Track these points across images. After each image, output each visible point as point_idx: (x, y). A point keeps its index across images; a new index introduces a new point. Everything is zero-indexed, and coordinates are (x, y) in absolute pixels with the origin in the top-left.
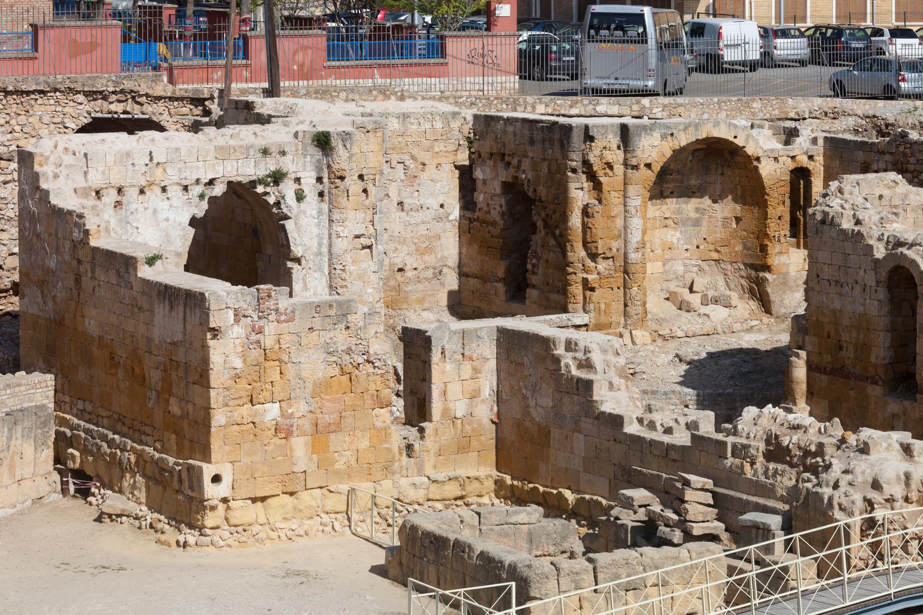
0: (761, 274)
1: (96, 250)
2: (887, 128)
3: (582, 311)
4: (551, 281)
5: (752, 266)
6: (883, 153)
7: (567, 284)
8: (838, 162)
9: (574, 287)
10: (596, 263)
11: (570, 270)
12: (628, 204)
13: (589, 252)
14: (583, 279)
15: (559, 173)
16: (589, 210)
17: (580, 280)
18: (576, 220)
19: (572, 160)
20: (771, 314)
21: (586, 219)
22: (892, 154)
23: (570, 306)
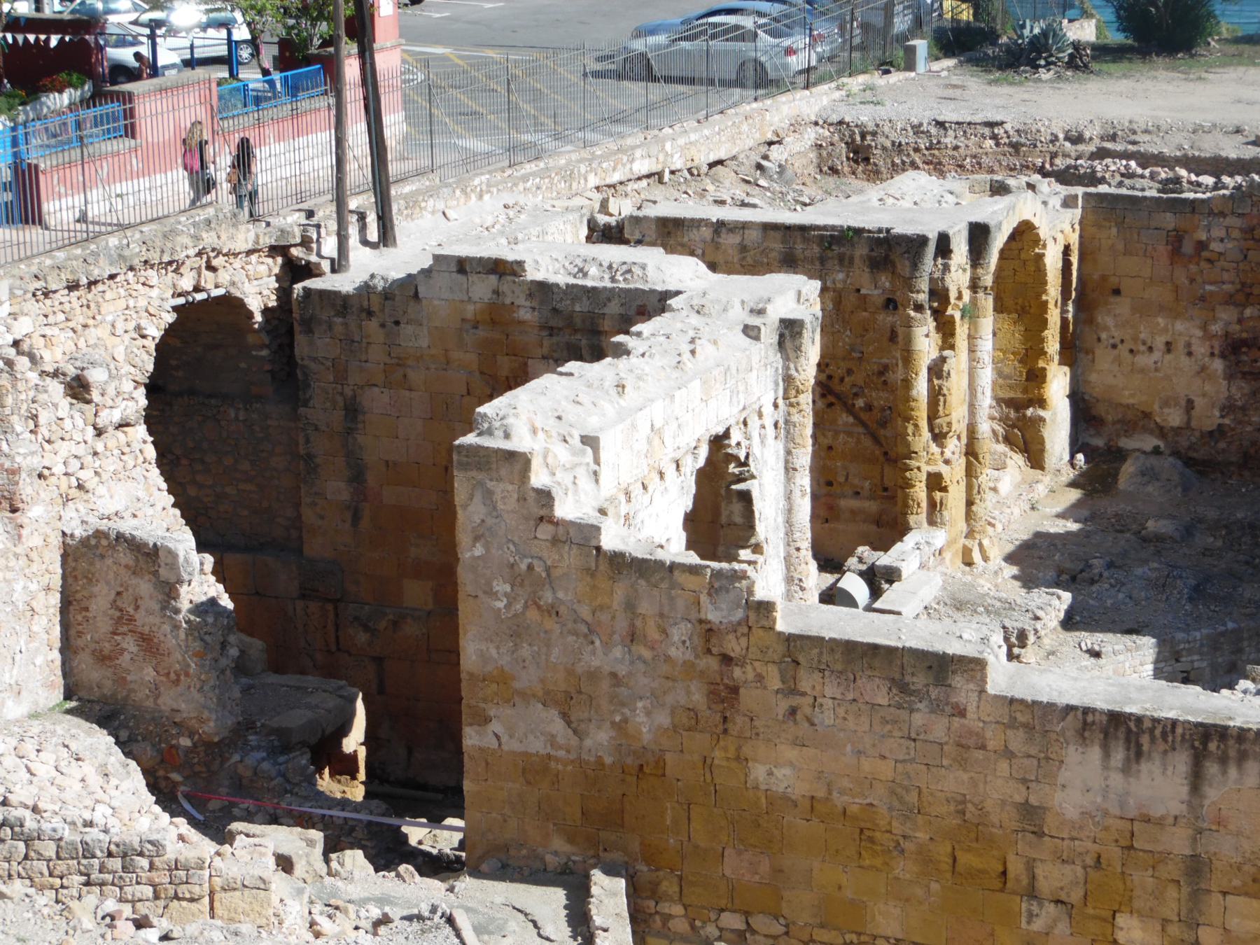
0: (1030, 412)
1: (790, 639)
2: (863, 137)
3: (925, 524)
4: (842, 479)
5: (1010, 403)
6: (1222, 214)
7: (908, 484)
8: (1114, 231)
9: (917, 489)
10: (941, 446)
11: (913, 463)
12: (979, 348)
13: (937, 431)
14: (929, 475)
15: (865, 310)
16: (946, 368)
17: (924, 478)
18: (921, 387)
19: (918, 292)
20: (1042, 468)
21: (936, 382)
22: (1240, 215)
23: (912, 519)
